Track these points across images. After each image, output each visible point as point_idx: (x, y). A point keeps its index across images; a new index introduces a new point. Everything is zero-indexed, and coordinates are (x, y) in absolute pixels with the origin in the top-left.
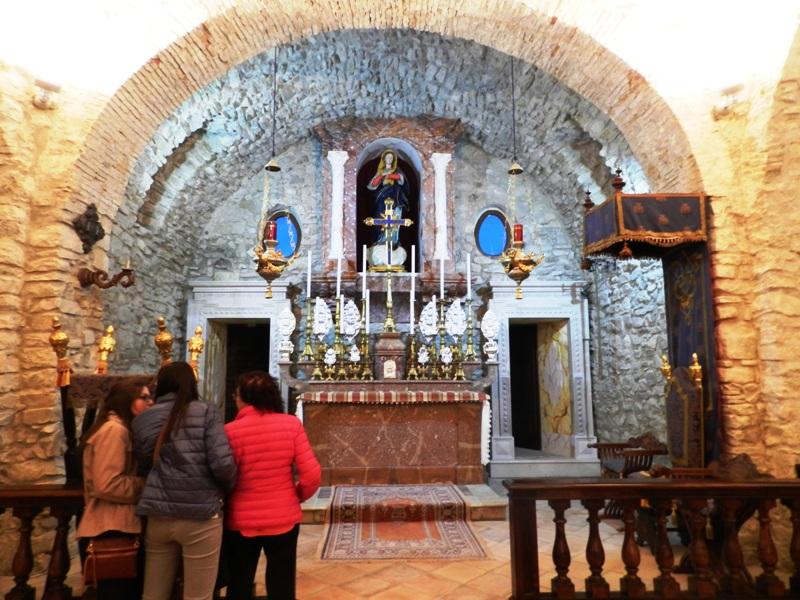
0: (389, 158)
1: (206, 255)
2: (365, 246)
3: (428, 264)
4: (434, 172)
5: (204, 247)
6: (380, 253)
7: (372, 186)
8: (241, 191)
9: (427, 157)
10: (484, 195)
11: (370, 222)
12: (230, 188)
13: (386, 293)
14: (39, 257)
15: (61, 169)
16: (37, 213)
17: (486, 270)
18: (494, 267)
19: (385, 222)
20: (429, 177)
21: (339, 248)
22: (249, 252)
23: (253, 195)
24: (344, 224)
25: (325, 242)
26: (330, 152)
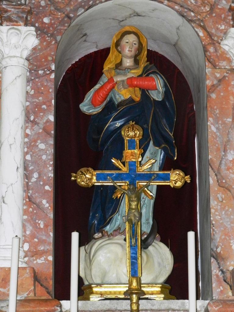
0: (129, 44)
2: (75, 236)
6: (106, 261)
11: (88, 178)
20: (220, 81)
24: (27, 187)
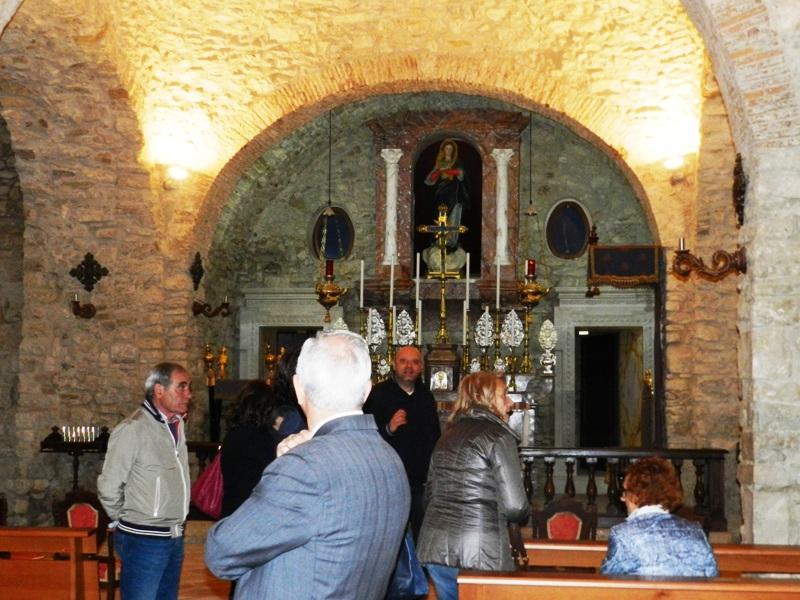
1: (255, 259)
3: (488, 269)
4: (495, 168)
5: (253, 250)
7: (429, 182)
8: (289, 188)
9: (488, 152)
10: (556, 188)
12: (280, 186)
13: (440, 301)
14: (171, 297)
15: (183, 234)
16: (169, 264)
17: (555, 273)
18: (565, 269)
19: (438, 229)
20: (490, 173)
21: (391, 256)
22: (299, 256)
23: (302, 192)
24: (398, 227)
25: (380, 245)
26: (383, 150)
